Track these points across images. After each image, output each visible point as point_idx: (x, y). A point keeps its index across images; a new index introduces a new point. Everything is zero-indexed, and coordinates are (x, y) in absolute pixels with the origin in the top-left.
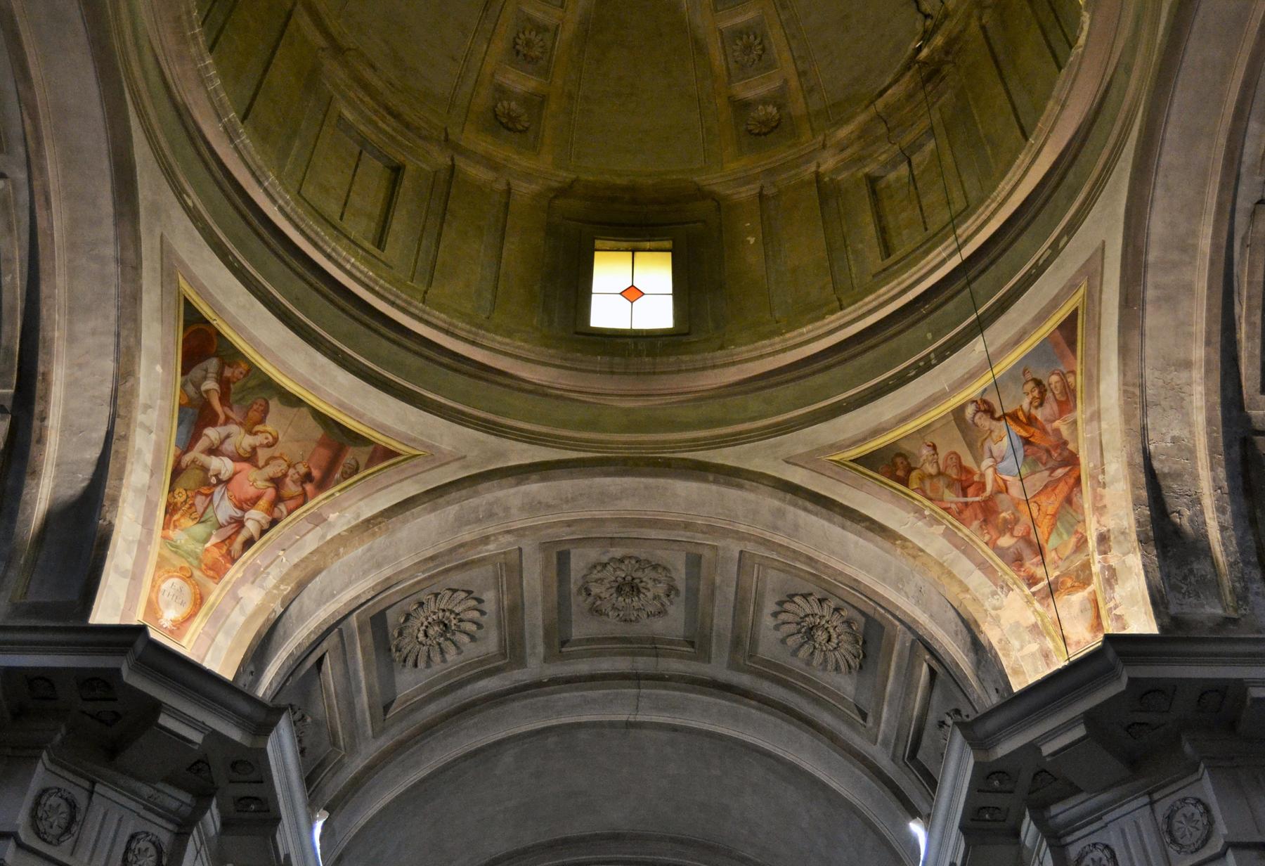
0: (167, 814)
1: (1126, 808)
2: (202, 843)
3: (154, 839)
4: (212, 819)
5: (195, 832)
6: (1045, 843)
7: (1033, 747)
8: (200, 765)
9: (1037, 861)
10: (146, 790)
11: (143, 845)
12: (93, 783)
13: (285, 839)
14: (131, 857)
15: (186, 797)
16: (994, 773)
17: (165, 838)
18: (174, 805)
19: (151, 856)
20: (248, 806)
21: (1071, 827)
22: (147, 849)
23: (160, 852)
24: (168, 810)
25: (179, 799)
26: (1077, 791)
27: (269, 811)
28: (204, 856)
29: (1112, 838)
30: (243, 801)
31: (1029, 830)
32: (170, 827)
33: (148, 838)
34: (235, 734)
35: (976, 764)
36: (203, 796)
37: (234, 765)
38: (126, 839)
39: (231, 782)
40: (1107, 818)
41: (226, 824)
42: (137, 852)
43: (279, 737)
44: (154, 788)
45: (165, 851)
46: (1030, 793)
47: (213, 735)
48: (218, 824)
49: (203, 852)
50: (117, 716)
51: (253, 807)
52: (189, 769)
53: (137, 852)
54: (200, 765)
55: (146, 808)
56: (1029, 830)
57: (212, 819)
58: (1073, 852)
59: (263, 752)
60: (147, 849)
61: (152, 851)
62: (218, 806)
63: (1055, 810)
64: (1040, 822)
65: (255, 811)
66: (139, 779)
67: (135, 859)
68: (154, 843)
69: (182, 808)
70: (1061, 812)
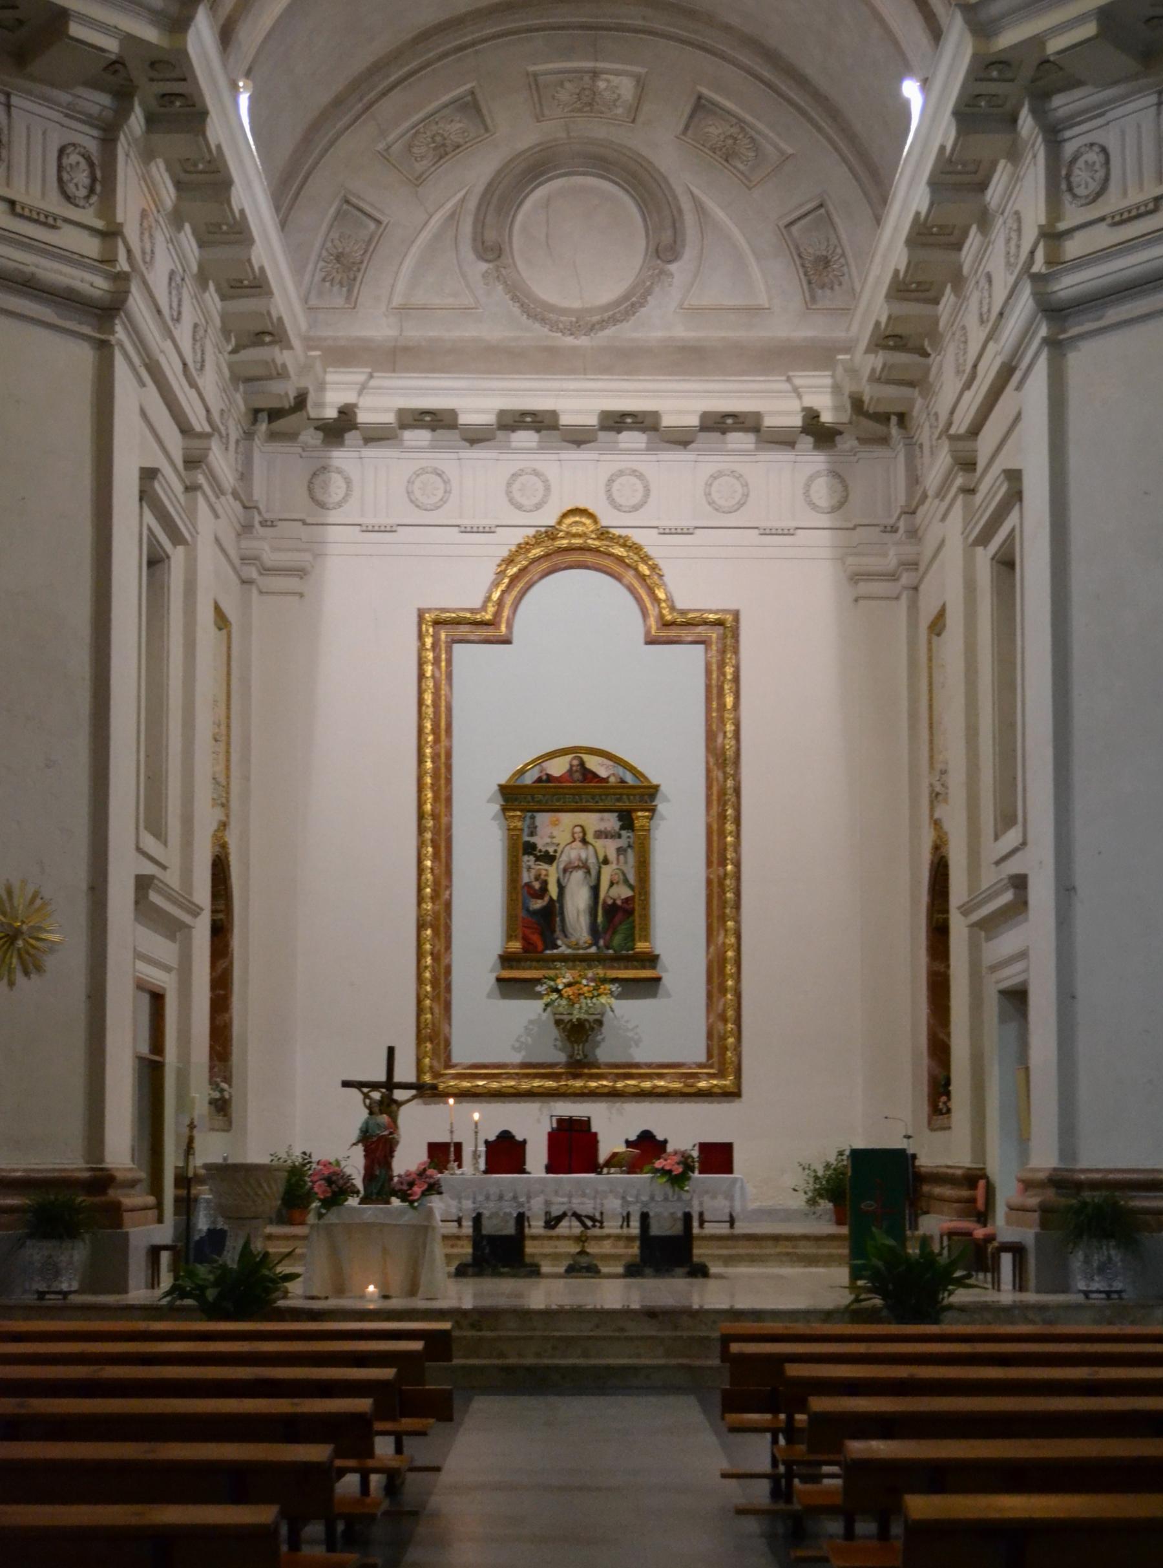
0: (90, 120)
1: (1131, 107)
2: (129, 144)
3: (82, 150)
4: (136, 121)
5: (122, 137)
6: (1040, 139)
7: (1038, 41)
8: (116, 65)
9: (1030, 156)
10: (64, 97)
11: (73, 158)
12: (8, 95)
13: (215, 131)
14: (66, 177)
15: (105, 99)
16: (993, 63)
17: (92, 146)
18: (95, 110)
19: (84, 170)
20: (172, 103)
21: (1071, 121)
22: (78, 163)
23: (91, 164)
24: (90, 116)
25: (99, 101)
26: (1079, 83)
27: (194, 106)
28: (133, 158)
29: (1111, 139)
30: (167, 98)
31: (1026, 123)
32: (95, 133)
33: (77, 151)
34: (150, 34)
35: (975, 56)
36: (123, 95)
37: (153, 64)
38: (55, 154)
39: (152, 80)
40: (1110, 115)
41: (151, 120)
42: (69, 169)
43: (198, 33)
44: (74, 95)
45: (96, 162)
46: (1033, 81)
47: (129, 39)
48: (142, 121)
49: (132, 154)
50: (20, 22)
51: (178, 104)
52: (106, 69)
53: (69, 169)
54: (117, 66)
55: (67, 115)
56: (1026, 123)
57: (136, 121)
58: (1069, 149)
59: (185, 53)
60: (78, 163)
61: (83, 164)
62: (140, 104)
63: (1058, 101)
64: (1039, 114)
65: (180, 106)
66: (53, 85)
67: (69, 178)
68: (83, 156)
69: (104, 113)
70: (1062, 104)
